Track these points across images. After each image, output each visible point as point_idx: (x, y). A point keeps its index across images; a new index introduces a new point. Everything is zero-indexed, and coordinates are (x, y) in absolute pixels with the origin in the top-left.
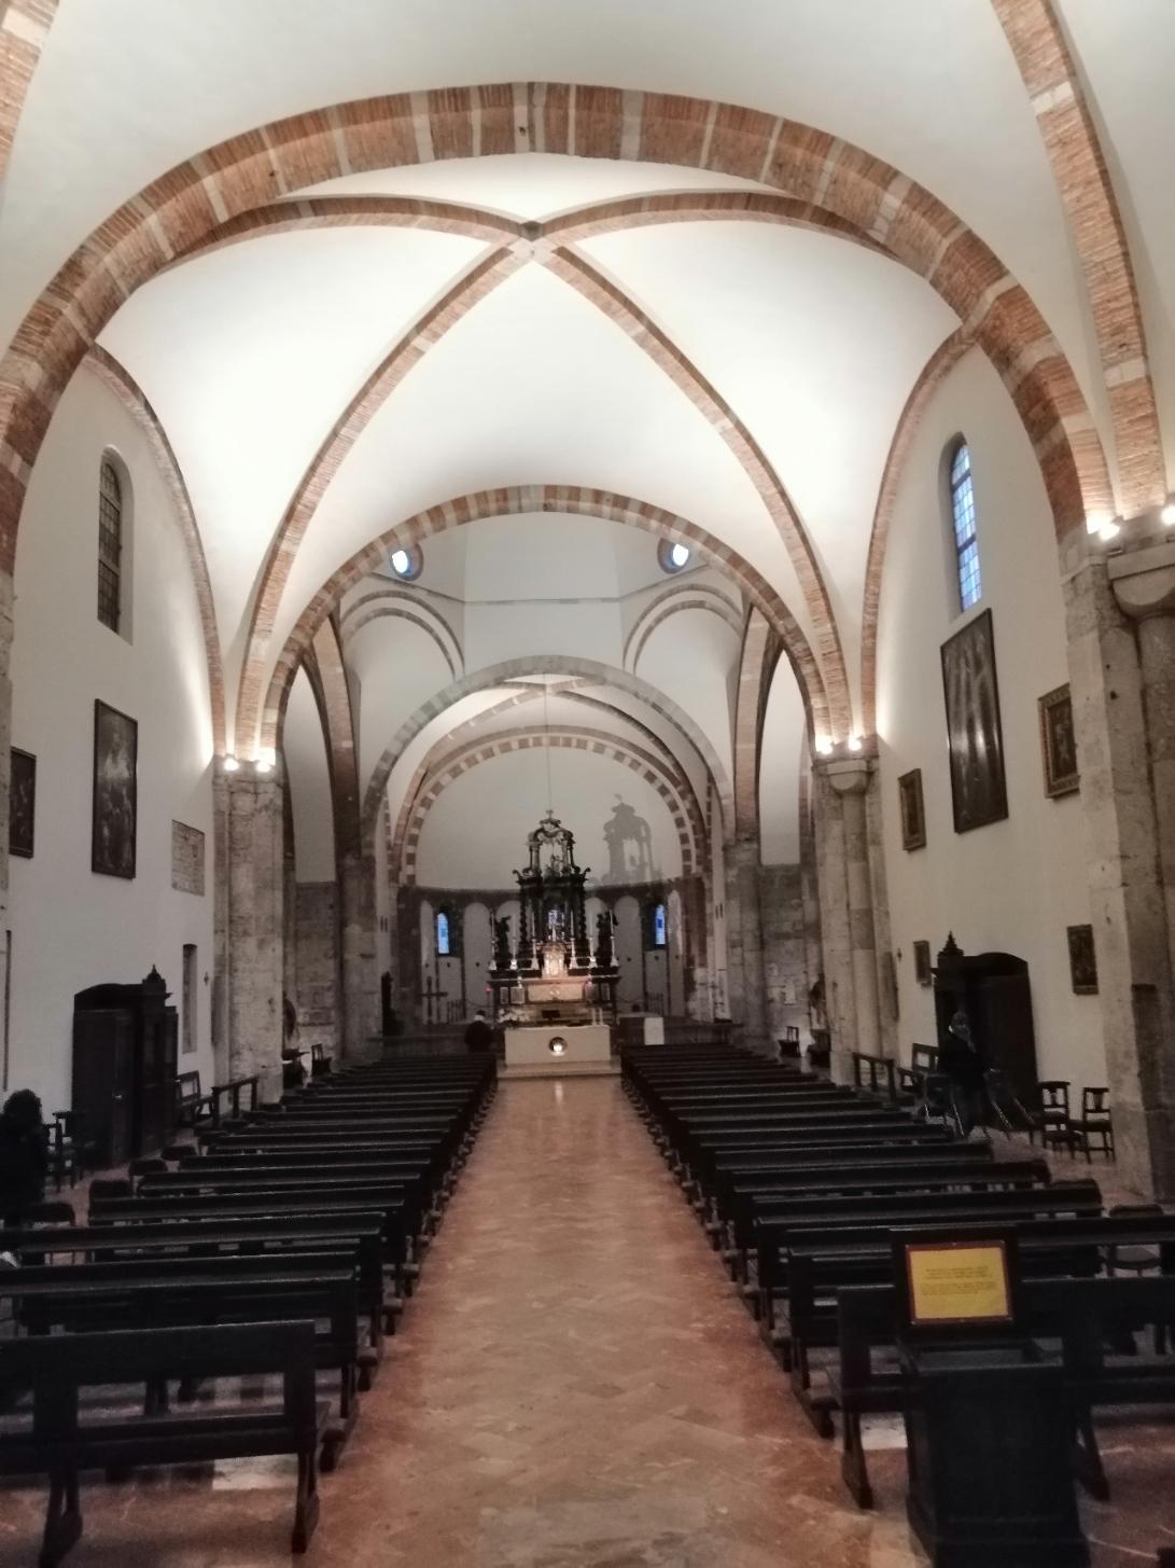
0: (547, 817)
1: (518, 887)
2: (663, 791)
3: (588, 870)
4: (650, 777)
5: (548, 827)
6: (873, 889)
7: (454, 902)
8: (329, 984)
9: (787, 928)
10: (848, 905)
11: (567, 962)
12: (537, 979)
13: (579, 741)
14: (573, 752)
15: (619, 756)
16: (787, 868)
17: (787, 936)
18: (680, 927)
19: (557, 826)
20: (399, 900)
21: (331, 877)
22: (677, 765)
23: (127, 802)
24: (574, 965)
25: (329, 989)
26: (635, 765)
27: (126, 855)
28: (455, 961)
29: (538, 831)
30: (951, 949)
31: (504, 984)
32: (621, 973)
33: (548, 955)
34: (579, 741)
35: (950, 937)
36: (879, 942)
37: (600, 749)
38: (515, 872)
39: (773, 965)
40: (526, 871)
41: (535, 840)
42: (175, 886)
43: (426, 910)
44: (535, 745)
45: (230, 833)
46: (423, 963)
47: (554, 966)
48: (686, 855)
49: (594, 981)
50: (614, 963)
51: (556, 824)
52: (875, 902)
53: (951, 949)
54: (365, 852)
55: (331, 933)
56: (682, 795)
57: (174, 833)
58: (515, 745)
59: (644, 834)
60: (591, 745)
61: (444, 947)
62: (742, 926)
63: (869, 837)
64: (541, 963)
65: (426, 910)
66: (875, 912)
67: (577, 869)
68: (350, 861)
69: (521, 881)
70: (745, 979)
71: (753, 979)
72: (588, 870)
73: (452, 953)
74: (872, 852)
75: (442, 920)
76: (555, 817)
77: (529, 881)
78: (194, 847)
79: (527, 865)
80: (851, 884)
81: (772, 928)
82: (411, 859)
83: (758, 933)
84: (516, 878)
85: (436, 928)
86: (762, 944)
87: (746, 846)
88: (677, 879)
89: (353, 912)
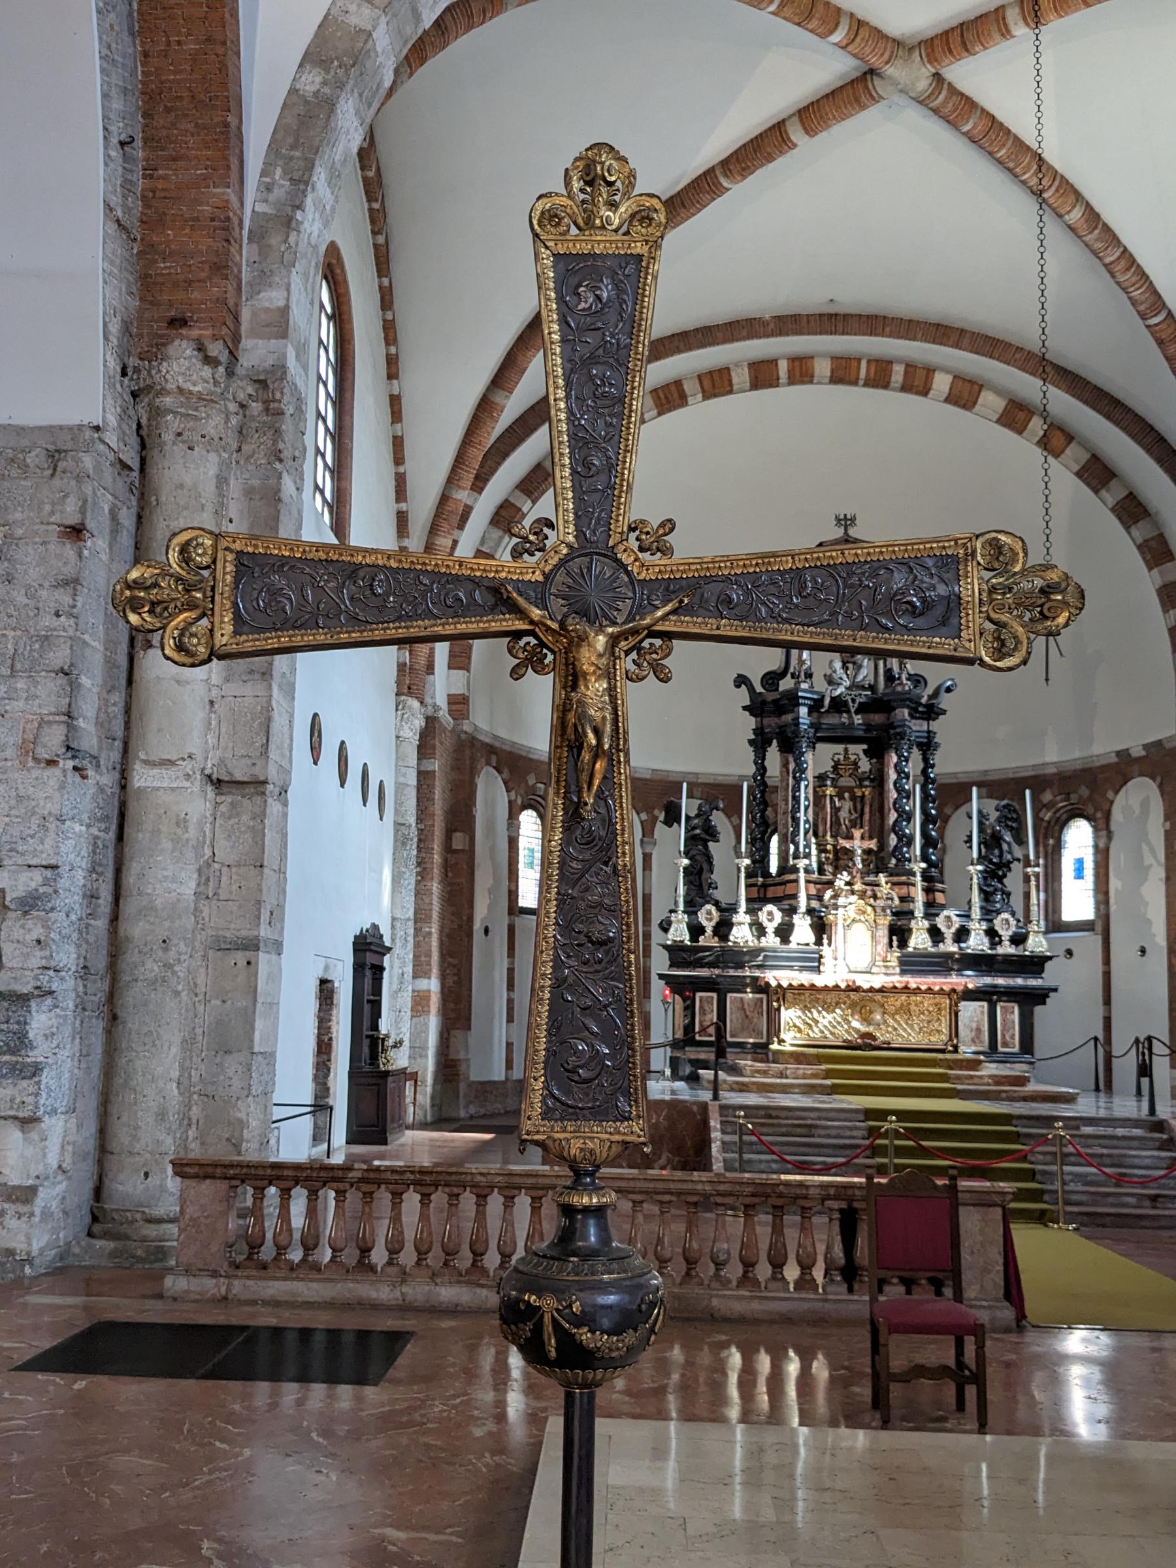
0: (839, 533)
11: (899, 933)
13: (910, 367)
14: (893, 404)
15: (1015, 415)
18: (1158, 873)
20: (425, 748)
31: (708, 985)
32: (1050, 976)
37: (964, 394)
43: (491, 791)
46: (478, 926)
54: (256, 352)
64: (821, 928)
65: (491, 791)
68: (182, 368)
85: (513, 842)
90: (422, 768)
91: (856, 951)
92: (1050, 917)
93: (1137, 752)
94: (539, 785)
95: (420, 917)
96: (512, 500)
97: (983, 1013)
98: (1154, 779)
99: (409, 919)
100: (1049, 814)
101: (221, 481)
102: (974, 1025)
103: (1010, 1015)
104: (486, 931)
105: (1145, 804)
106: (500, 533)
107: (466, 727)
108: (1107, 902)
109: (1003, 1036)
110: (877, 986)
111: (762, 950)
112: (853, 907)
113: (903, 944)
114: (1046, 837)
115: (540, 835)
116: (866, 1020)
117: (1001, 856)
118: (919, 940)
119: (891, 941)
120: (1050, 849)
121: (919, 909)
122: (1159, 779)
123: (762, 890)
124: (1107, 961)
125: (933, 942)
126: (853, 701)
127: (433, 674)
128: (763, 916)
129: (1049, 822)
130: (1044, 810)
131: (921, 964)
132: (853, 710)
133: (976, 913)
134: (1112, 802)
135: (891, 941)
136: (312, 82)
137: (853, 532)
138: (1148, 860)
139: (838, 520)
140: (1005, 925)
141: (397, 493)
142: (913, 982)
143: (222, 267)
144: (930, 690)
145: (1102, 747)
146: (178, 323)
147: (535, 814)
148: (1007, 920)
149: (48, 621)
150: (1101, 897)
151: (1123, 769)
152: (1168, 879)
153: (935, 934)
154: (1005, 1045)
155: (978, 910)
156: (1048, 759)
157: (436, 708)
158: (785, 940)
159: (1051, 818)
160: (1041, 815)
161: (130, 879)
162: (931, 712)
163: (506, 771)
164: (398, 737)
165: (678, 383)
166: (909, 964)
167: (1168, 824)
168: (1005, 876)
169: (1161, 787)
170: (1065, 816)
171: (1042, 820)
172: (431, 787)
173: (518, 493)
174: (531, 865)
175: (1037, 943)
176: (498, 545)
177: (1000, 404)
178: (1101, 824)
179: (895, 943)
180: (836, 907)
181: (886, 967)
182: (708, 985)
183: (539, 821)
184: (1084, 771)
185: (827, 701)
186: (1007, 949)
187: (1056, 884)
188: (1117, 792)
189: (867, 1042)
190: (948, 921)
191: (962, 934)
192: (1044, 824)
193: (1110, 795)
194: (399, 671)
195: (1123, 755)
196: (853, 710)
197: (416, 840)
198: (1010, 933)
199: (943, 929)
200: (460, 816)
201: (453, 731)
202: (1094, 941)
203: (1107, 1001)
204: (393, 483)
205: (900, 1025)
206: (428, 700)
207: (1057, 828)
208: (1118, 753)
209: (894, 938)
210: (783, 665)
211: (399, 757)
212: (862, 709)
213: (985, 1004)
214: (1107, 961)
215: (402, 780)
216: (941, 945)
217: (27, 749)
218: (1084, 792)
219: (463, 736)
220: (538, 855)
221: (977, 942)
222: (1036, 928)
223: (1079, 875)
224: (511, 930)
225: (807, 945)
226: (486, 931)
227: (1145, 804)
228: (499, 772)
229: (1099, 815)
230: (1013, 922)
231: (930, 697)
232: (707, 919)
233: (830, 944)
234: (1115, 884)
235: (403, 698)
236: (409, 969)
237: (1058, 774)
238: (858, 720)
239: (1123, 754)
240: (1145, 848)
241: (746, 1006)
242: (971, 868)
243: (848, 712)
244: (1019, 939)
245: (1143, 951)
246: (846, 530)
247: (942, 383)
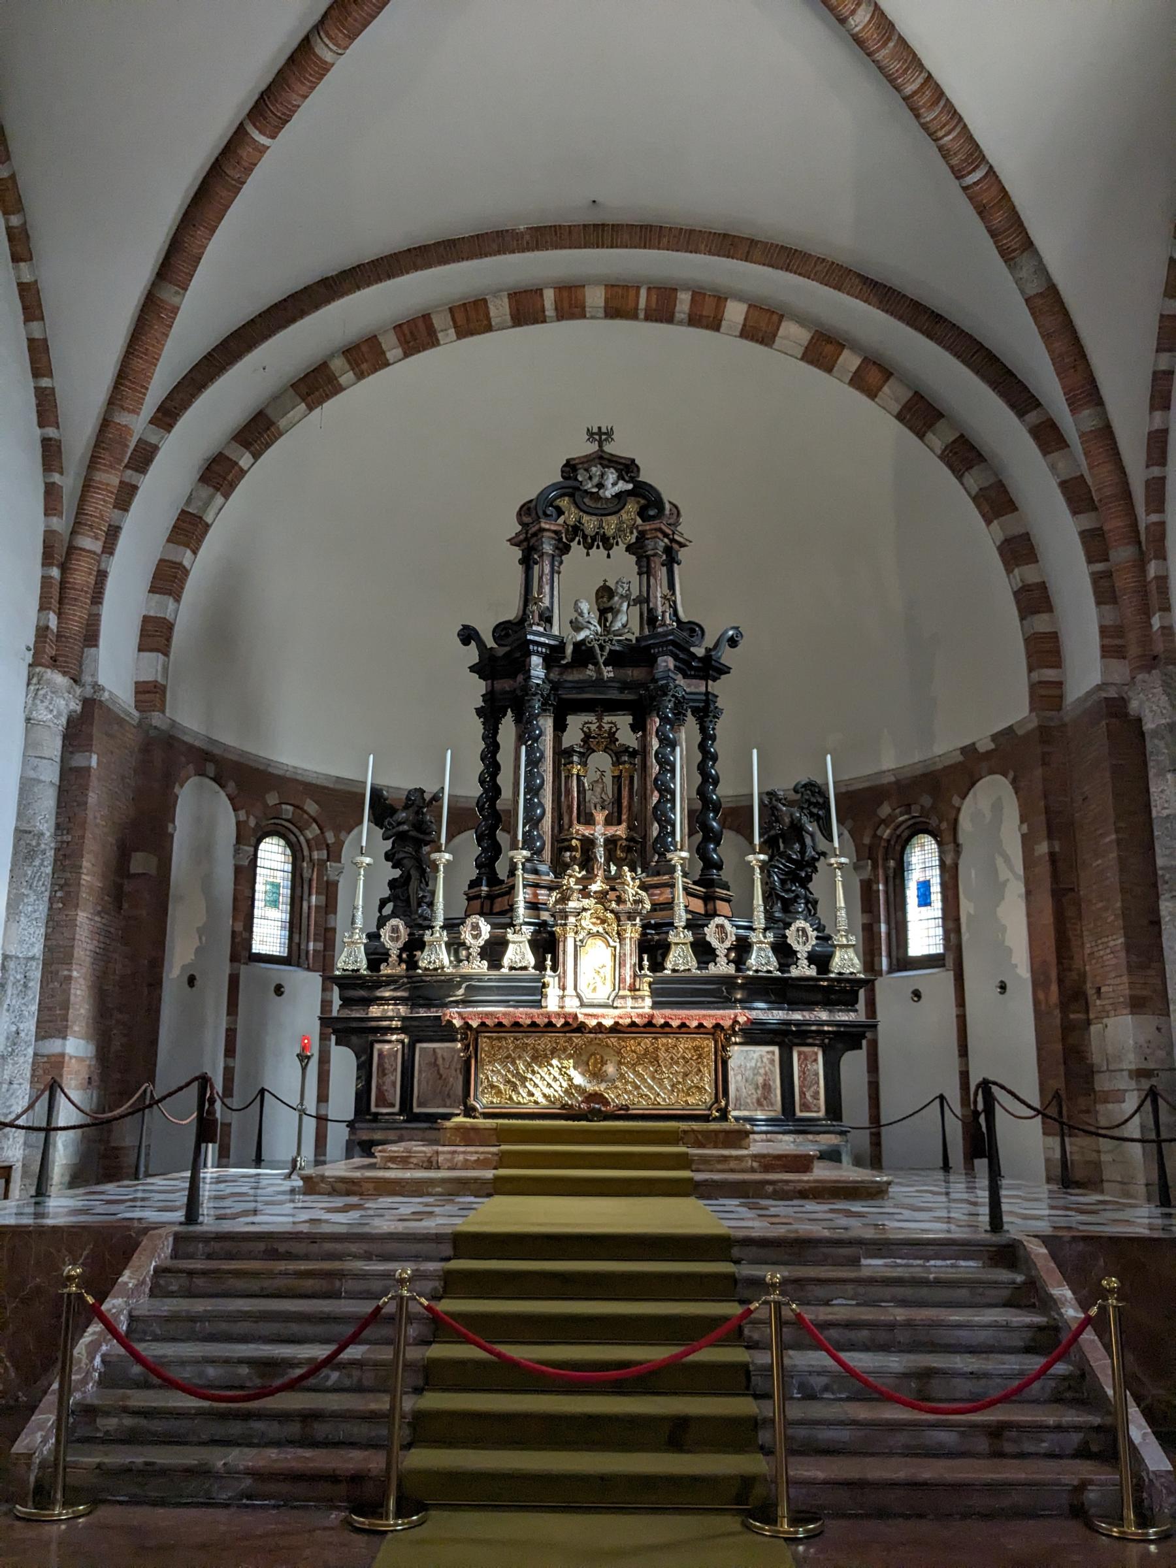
0: (594, 447)
7: (312, 807)
11: (653, 949)
18: (1016, 889)
22: (1049, 306)
40: (503, 630)
44: (561, 316)
46: (174, 972)
48: (1045, 650)
51: (627, 469)
56: (1048, 436)
61: (269, 933)
73: (294, 957)
75: (273, 858)
85: (246, 873)
90: (74, 764)
91: (595, 977)
92: (894, 953)
93: (985, 745)
94: (284, 806)
95: (56, 957)
96: (227, 453)
97: (772, 1061)
98: (1005, 775)
99: (33, 958)
100: (888, 831)
102: (760, 1080)
103: (811, 1065)
104: (191, 981)
105: (997, 808)
106: (211, 490)
107: (156, 719)
108: (958, 930)
109: (802, 1094)
110: (608, 1023)
111: (465, 978)
112: (587, 914)
113: (657, 966)
114: (886, 859)
115: (289, 867)
116: (597, 1075)
117: (803, 851)
118: (680, 959)
119: (641, 960)
120: (891, 873)
121: (681, 917)
122: (1011, 775)
123: (487, 903)
124: (961, 1002)
125: (699, 963)
126: (602, 648)
127: (96, 646)
128: (466, 935)
129: (888, 841)
130: (883, 826)
131: (684, 993)
132: (601, 661)
133: (760, 920)
134: (959, 810)
135: (641, 960)
137: (609, 448)
138: (1004, 873)
139: (590, 434)
140: (801, 936)
141: (40, 414)
142: (675, 1016)
144: (709, 641)
145: (945, 746)
147: (282, 842)
148: (804, 930)
150: (951, 925)
151: (968, 769)
152: (1028, 893)
153: (704, 952)
154: (805, 1107)
155: (762, 916)
156: (885, 768)
157: (97, 688)
158: (495, 964)
159: (891, 835)
160: (879, 833)
162: (710, 668)
163: (231, 785)
164: (28, 720)
165: (426, 318)
166: (664, 994)
167: (1025, 827)
168: (809, 879)
169: (1014, 782)
170: (906, 834)
171: (881, 838)
172: (84, 789)
173: (235, 445)
174: (274, 904)
175: (847, 961)
176: (207, 504)
178: (947, 837)
179: (646, 963)
180: (565, 915)
181: (634, 998)
183: (288, 851)
184: (924, 775)
185: (569, 649)
186: (803, 969)
187: (899, 914)
188: (964, 798)
189: (594, 1107)
190: (721, 933)
191: (742, 948)
192: (883, 844)
193: (956, 800)
194: (38, 636)
195: (969, 751)
196: (601, 661)
197: (50, 854)
198: (809, 948)
199: (715, 943)
200: (145, 832)
201: (140, 725)
202: (943, 978)
203: (963, 1051)
204: (33, 401)
205: (644, 1080)
206: (87, 678)
207: (898, 848)
208: (963, 750)
209: (645, 957)
210: (521, 613)
211: (30, 744)
212: (615, 659)
213: (776, 1049)
214: (961, 1002)
215: (32, 774)
216: (711, 965)
218: (927, 801)
219: (152, 733)
220: (286, 892)
221: (761, 960)
222: (844, 941)
223: (925, 901)
224: (234, 981)
225: (525, 968)
226: (191, 981)
227: (997, 808)
228: (222, 786)
229: (944, 826)
230: (813, 934)
231: (708, 650)
232: (392, 939)
233: (554, 968)
234: (966, 907)
235: (38, 669)
237: (897, 782)
238: (608, 672)
240: (1000, 861)
241: (440, 1061)
242: (751, 857)
243: (596, 664)
244: (821, 960)
245: (1003, 987)
246: (600, 446)
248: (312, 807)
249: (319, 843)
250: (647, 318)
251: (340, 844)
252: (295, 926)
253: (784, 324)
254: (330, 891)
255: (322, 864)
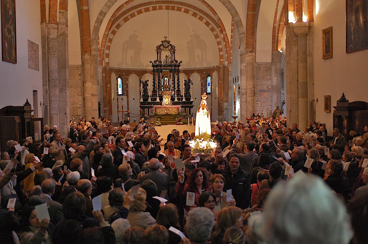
1: (152, 68)
2: (213, 30)
3: (181, 62)
4: (207, 24)
5: (164, 44)
6: (308, 74)
7: (124, 73)
8: (80, 106)
9: (265, 88)
10: (298, 81)
12: (160, 106)
13: (178, 7)
16: (266, 64)
17: (264, 91)
19: (168, 44)
21: (80, 63)
22: (219, 19)
23: (13, 32)
24: (176, 100)
25: (79, 108)
26: (201, 19)
27: (13, 54)
28: (125, 97)
29: (161, 45)
30: (343, 99)
31: (146, 107)
32: (193, 104)
33: (164, 96)
34: (178, 7)
35: (343, 95)
36: (309, 96)
38: (151, 62)
39: (258, 102)
40: (155, 62)
41: (159, 49)
42: (29, 67)
43: (113, 76)
44: (159, 9)
45: (48, 45)
46: (112, 98)
47: (166, 100)
48: (221, 57)
49: (182, 107)
50: (192, 100)
52: (308, 79)
53: (343, 99)
55: (80, 86)
57: (28, 45)
58: (151, 9)
59: (203, 47)
60: (183, 10)
62: (247, 87)
63: (308, 54)
65: (113, 76)
66: (308, 83)
67: (177, 61)
68: (87, 56)
69: (153, 66)
70: (247, 108)
71: (250, 108)
72: (181, 62)
74: (309, 59)
76: (167, 39)
77: (157, 66)
78: (35, 51)
79: (156, 59)
80: (299, 72)
81: (259, 87)
82: (108, 56)
83: (253, 89)
84: (151, 64)
86: (254, 94)
87: (250, 54)
88: (217, 66)
89: (88, 77)
101: (91, 66)
136: (96, 24)
143: (90, 46)
144: (178, 63)
146: (86, 52)
149: (79, 83)
161: (86, 104)
177: (192, 13)
182: (146, 107)
217: (78, 94)
220: (121, 85)
224: (118, 98)
236: (103, 107)
239: (214, 67)
247: (183, 10)
248: (124, 73)
249: (125, 78)
250: (171, 10)
251: (128, 78)
252: (123, 90)
253: (189, 11)
254: (127, 85)
255: (126, 81)
